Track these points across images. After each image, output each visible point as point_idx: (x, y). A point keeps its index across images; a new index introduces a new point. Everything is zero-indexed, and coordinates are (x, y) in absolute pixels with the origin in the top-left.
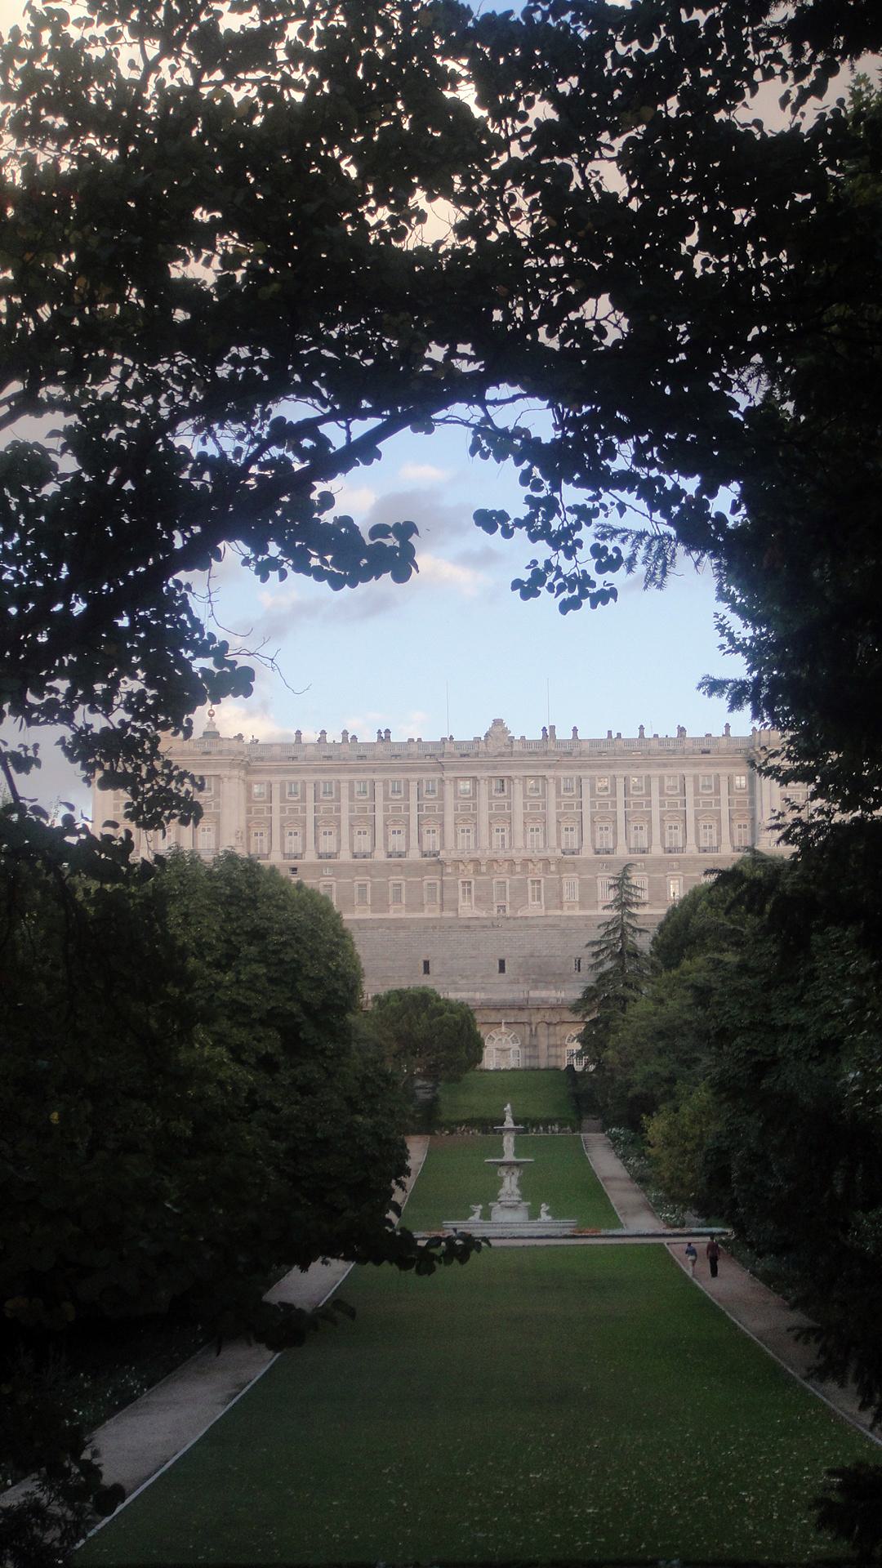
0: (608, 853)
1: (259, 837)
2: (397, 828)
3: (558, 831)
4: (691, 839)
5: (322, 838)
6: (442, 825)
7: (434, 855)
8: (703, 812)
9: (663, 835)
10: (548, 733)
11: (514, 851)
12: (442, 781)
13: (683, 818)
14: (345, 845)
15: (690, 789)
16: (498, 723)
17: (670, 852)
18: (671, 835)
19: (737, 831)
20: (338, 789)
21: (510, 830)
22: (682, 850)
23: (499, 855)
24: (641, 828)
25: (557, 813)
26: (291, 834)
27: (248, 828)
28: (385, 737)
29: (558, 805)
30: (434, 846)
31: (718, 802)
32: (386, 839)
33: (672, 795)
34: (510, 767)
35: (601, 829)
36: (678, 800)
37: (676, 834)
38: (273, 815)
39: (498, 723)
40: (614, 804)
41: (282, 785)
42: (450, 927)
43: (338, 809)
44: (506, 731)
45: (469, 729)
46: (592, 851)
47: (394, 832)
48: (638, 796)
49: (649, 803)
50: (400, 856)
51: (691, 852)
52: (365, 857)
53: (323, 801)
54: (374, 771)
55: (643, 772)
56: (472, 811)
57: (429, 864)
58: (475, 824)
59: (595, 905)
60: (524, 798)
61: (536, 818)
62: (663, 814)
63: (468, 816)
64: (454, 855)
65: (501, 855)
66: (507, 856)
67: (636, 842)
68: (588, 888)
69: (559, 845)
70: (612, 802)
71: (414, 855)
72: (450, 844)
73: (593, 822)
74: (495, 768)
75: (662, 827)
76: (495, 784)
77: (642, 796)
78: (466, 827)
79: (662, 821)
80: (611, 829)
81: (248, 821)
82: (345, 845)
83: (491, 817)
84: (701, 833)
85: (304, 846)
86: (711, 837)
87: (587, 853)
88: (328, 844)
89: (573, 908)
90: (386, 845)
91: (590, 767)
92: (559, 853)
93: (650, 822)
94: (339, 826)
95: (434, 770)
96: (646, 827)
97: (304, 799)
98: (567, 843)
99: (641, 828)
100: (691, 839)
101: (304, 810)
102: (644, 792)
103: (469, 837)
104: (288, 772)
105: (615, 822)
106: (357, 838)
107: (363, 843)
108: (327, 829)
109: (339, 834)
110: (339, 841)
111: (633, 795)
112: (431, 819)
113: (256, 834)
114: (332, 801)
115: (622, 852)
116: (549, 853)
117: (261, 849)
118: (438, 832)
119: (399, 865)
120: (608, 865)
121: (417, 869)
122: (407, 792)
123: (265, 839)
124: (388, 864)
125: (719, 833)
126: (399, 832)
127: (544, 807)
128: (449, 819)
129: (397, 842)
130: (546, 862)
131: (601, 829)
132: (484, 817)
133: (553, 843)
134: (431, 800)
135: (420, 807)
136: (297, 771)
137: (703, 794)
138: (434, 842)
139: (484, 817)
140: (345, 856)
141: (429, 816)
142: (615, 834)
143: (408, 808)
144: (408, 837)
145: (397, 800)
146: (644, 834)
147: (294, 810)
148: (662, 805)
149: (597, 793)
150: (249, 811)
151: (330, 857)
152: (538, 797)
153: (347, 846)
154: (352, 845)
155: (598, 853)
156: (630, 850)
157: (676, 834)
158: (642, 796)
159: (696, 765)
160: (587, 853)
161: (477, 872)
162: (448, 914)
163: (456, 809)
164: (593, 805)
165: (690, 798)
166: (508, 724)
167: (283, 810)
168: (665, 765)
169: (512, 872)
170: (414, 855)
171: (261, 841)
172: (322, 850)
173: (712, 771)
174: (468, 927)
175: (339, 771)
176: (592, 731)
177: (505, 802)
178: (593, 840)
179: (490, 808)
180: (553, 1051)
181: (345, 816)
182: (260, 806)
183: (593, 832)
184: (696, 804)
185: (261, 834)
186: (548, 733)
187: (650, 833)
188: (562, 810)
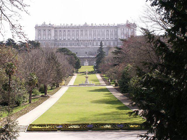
10: (92, 24)
14: (67, 38)
28: (72, 24)
39: (86, 23)
45: (82, 24)
59: (98, 46)
61: (90, 35)
63: (82, 35)
64: (80, 39)
68: (97, 43)
71: (75, 39)
72: (80, 38)
76: (85, 30)
82: (67, 38)
87: (97, 39)
88: (65, 38)
89: (95, 46)
97: (62, 32)
115: (101, 39)
120: (99, 41)
121: (76, 41)
128: (80, 35)
129: (73, 38)
130: (92, 40)
132: (84, 35)
133: (93, 38)
136: (61, 29)
139: (84, 35)
140: (67, 39)
159: (110, 28)
160: (97, 39)
161: (83, 41)
162: (80, 47)
169: (87, 41)
170: (75, 39)
176: (98, 24)
180: (92, 63)
186: (92, 24)
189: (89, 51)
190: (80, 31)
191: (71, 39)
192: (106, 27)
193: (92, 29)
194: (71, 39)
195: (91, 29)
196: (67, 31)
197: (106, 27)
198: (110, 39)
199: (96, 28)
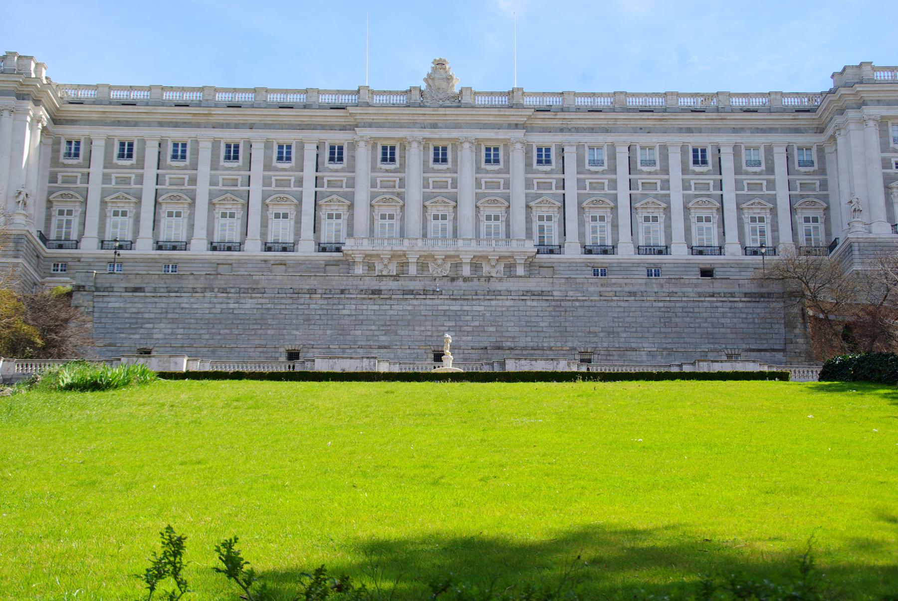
0: (605, 252)
1: (65, 218)
2: (281, 210)
3: (529, 220)
4: (732, 235)
5: (164, 221)
6: (351, 207)
7: (338, 250)
8: (749, 198)
9: (688, 230)
11: (460, 243)
12: (353, 145)
13: (718, 205)
14: (200, 232)
15: (728, 163)
16: (440, 64)
17: (701, 253)
18: (700, 229)
19: (802, 228)
20: (196, 152)
21: (455, 219)
22: (720, 250)
23: (437, 248)
24: (655, 219)
25: (527, 195)
26: (116, 214)
27: (50, 202)
29: (528, 184)
30: (337, 236)
31: (771, 185)
32: (264, 224)
33: (701, 173)
34: (457, 126)
35: (594, 219)
36: (711, 180)
37: (708, 229)
38: (91, 186)
39: (440, 64)
40: (614, 184)
41: (109, 141)
42: (342, 292)
43: (193, 181)
44: (449, 79)
46: (579, 249)
47: (277, 216)
48: (650, 173)
49: (666, 184)
50: (284, 249)
51: (733, 254)
52: (229, 249)
53: (171, 168)
54: (251, 127)
55: (655, 139)
56: (397, 190)
57: (328, 264)
58: (402, 207)
60: (477, 172)
62: (687, 200)
64: (366, 246)
65: (440, 248)
66: (450, 249)
67: (647, 239)
69: (529, 235)
70: (610, 181)
71: (307, 249)
73: (581, 209)
74: (434, 126)
75: (687, 219)
77: (655, 173)
78: (387, 211)
79: (686, 209)
80: (608, 219)
81: (50, 193)
82: (200, 232)
83: (426, 197)
84: (748, 228)
85: (136, 232)
86: (762, 233)
87: (573, 252)
88: (172, 230)
90: (264, 234)
91: (578, 130)
92: (530, 247)
93: (667, 210)
94: (192, 205)
95: (343, 128)
96: (662, 218)
98: (541, 238)
99: (655, 219)
100: (732, 235)
101: (140, 180)
102: (658, 167)
103: (391, 225)
104: (118, 123)
105: (614, 209)
106: (219, 222)
107: (229, 230)
108: (174, 209)
109: (191, 217)
110: (191, 227)
111: (641, 172)
112: (334, 197)
113: (61, 213)
114: (185, 168)
116: (514, 246)
117: (68, 234)
118: (345, 216)
119: (282, 263)
122: (301, 158)
123: (76, 221)
124: (266, 261)
125: (775, 229)
126: (285, 216)
127: (507, 185)
128: (362, 197)
129: (281, 231)
131: (594, 219)
134: (336, 171)
135: (318, 181)
137: (747, 173)
138: (338, 231)
141: (332, 193)
142: (615, 226)
143: (300, 182)
144: (298, 222)
145: (285, 170)
146: (658, 229)
147: (126, 181)
148: (686, 186)
149: (587, 167)
150: (53, 179)
151: (174, 248)
152: (499, 172)
153: (204, 234)
154: (210, 232)
155: (590, 252)
156: (638, 250)
157: (708, 229)
158: (655, 173)
159: (735, 130)
160: (573, 252)
163: (373, 185)
164: (580, 184)
165: (728, 177)
166: (453, 69)
167: (106, 178)
168: (689, 130)
171: (69, 222)
172: (163, 237)
173: (761, 140)
174: (378, 292)
175: (198, 126)
177: (448, 178)
178: (582, 235)
179: (426, 185)
181: (203, 190)
182: (70, 172)
183: (581, 223)
184: (738, 185)
185: (70, 213)
187: (668, 227)
188: (535, 190)
189: (486, 341)
190: (363, 157)
191: (253, 248)
192: (690, 120)
193: (519, 134)
194: (253, 248)
195: (502, 134)
196: (205, 154)
197: (690, 120)
198: (733, 250)
199: (562, 130)
